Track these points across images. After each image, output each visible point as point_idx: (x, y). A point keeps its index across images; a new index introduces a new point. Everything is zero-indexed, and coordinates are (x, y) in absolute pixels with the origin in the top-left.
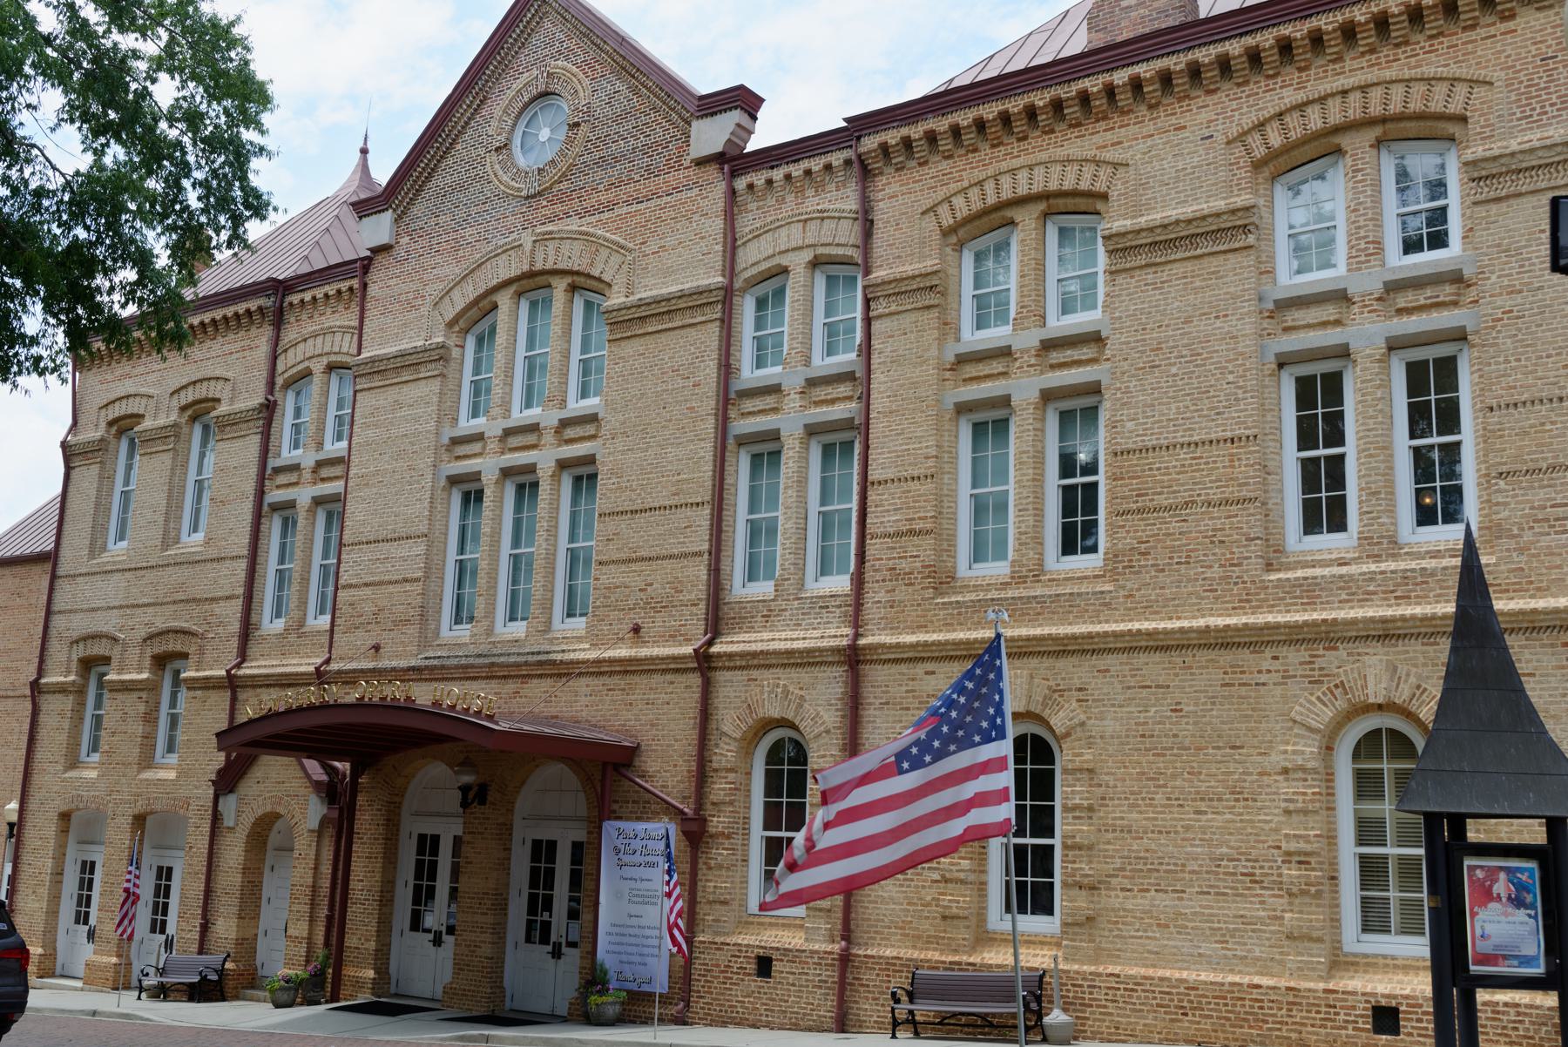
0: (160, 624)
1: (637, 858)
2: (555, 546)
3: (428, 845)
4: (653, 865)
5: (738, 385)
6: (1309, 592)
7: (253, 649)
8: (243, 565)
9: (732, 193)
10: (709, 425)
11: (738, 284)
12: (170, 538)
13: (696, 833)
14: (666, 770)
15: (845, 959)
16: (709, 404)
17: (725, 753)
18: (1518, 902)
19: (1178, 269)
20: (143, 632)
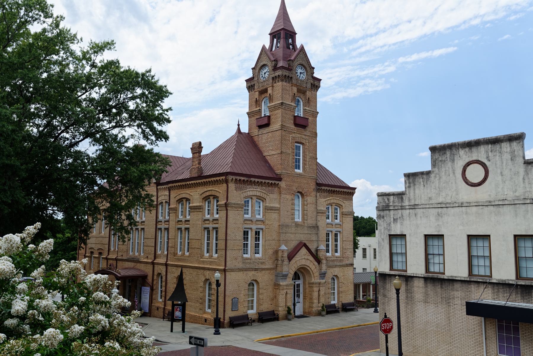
0: (99, 247)
3: (130, 287)
5: (158, 220)
6: (203, 262)
8: (108, 239)
9: (157, 189)
10: (155, 226)
12: (100, 232)
13: (152, 289)
14: (150, 279)
15: (164, 309)
16: (155, 223)
17: (155, 277)
20: (97, 248)
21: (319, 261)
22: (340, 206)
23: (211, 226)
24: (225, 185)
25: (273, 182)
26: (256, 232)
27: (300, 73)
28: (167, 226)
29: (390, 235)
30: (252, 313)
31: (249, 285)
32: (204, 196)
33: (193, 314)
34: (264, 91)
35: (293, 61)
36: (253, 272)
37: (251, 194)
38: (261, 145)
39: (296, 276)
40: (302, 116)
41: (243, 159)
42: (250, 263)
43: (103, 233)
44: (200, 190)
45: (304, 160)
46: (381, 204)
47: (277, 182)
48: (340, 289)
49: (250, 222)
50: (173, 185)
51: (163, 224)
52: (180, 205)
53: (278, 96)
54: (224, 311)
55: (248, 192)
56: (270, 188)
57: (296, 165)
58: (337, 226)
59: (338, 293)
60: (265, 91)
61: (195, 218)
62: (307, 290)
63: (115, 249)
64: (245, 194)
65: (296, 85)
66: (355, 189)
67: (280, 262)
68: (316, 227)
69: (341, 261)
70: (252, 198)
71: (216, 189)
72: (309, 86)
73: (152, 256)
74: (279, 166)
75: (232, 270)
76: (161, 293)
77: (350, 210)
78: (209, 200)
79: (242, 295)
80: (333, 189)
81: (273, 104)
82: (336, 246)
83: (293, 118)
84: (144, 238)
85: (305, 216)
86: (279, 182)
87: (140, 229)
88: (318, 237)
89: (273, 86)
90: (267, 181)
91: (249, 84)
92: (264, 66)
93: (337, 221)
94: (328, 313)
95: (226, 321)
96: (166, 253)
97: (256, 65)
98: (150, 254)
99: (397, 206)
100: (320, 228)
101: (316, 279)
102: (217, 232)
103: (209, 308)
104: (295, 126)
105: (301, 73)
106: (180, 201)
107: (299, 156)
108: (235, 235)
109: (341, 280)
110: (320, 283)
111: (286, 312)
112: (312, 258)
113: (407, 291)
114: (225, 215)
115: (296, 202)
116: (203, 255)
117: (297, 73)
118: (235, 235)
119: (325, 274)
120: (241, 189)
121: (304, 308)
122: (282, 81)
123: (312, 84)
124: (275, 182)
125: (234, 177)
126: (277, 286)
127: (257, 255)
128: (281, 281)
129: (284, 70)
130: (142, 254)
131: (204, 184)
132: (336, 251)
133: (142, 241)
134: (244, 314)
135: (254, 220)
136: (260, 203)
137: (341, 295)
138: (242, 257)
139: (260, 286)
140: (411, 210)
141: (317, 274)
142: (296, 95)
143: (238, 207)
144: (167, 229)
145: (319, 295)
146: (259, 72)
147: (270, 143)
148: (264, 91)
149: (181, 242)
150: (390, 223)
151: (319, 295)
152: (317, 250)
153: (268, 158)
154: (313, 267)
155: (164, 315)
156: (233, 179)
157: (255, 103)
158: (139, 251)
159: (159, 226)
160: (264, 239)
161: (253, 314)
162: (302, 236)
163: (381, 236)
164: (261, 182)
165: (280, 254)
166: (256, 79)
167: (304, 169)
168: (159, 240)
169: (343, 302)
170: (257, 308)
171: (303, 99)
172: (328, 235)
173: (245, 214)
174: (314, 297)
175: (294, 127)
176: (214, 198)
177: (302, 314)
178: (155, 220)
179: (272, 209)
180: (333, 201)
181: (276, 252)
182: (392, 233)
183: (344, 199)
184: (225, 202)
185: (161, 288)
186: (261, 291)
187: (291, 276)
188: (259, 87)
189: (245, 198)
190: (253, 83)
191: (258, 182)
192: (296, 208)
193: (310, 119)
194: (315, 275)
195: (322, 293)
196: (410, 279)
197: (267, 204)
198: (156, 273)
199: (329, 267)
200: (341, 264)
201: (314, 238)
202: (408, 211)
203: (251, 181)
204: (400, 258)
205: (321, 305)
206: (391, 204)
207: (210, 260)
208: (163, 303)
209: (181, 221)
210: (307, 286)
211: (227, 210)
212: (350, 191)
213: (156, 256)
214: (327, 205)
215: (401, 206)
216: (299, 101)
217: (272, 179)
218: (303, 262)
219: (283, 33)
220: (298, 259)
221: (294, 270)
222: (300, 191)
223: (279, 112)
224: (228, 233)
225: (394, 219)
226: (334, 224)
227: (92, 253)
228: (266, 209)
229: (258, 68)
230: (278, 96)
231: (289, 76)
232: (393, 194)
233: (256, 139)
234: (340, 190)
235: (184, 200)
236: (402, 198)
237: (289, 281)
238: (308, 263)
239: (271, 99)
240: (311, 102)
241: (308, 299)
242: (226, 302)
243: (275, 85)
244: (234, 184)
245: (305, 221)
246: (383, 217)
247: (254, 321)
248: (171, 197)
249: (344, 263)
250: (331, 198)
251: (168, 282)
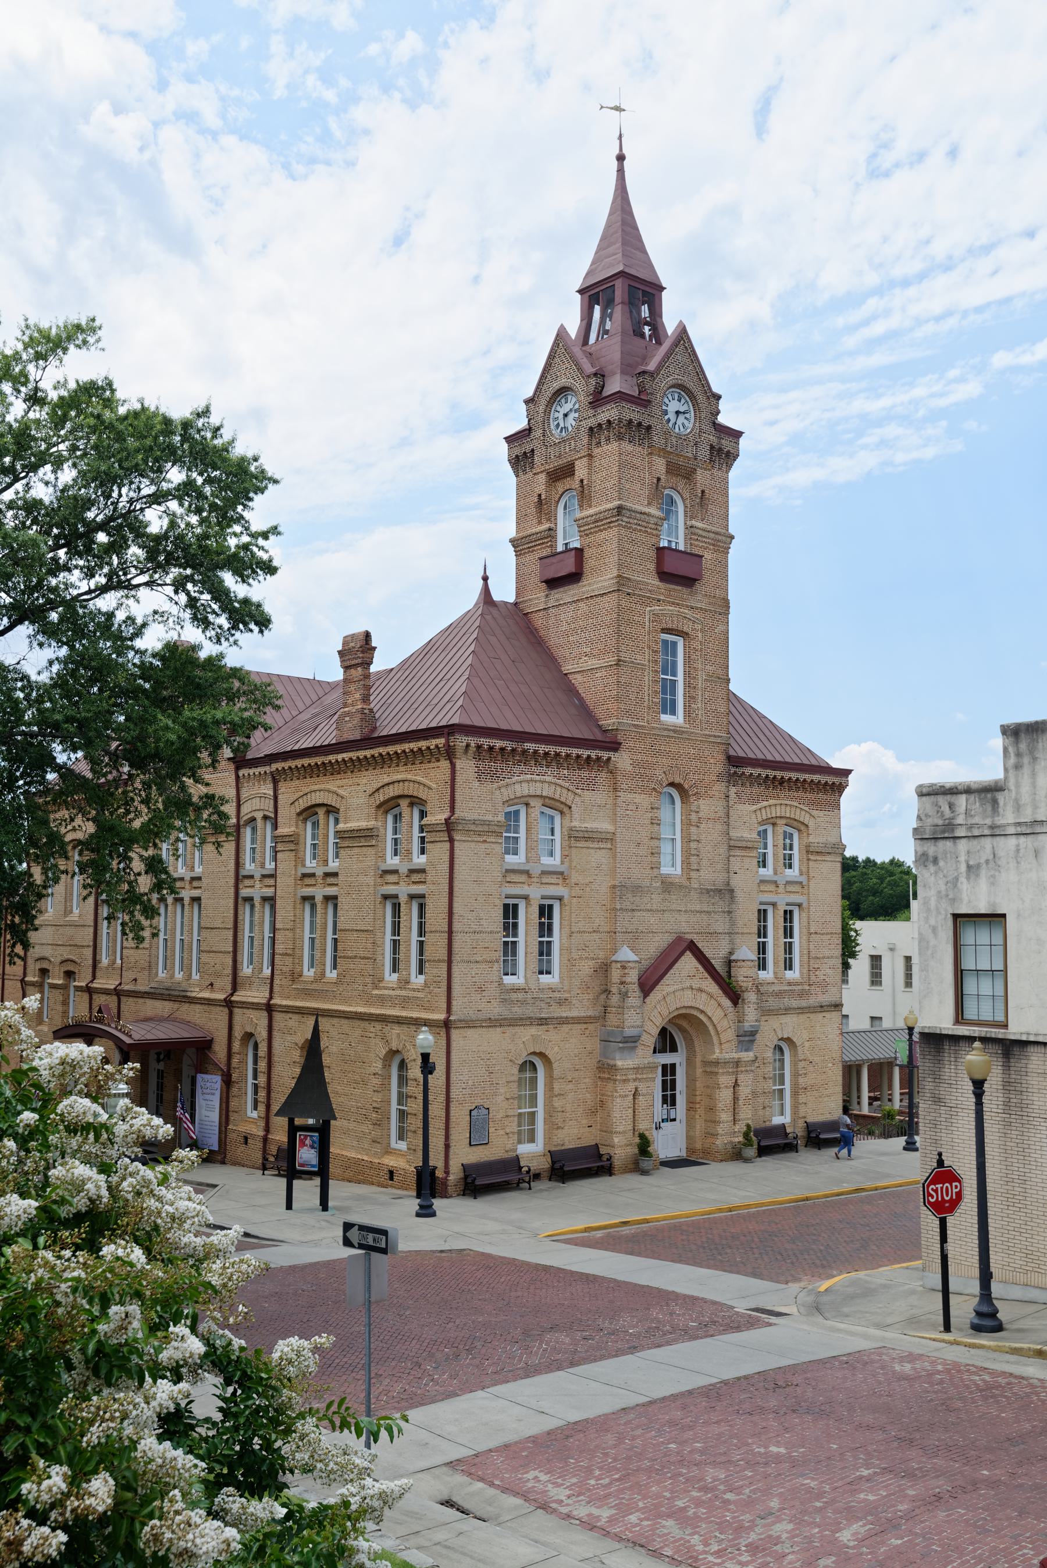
1: (208, 1091)
2: (192, 938)
3: (161, 1074)
4: (213, 1094)
5: (243, 872)
6: (382, 1000)
7: (98, 974)
8: (92, 930)
9: (237, 777)
10: (232, 890)
11: (242, 823)
12: (68, 911)
13: (228, 1082)
14: (219, 1051)
15: (265, 1140)
16: (232, 881)
17: (236, 1046)
18: (312, 1147)
19: (357, 850)
20: (59, 959)
21: (735, 996)
22: (801, 826)
23: (403, 890)
24: (445, 764)
25: (593, 754)
26: (542, 908)
27: (676, 413)
28: (269, 892)
29: (956, 916)
30: (532, 1152)
31: (522, 1067)
32: (381, 797)
33: (352, 1154)
34: (563, 473)
35: (652, 375)
36: (534, 1030)
37: (526, 792)
38: (554, 640)
39: (666, 1042)
40: (681, 547)
41: (500, 683)
42: (523, 1002)
43: (76, 911)
44: (370, 780)
45: (688, 685)
46: (929, 821)
47: (605, 755)
48: (801, 1080)
49: (523, 878)
50: (286, 765)
51: (258, 885)
52: (309, 825)
53: (609, 485)
54: (447, 1147)
55: (517, 786)
56: (585, 774)
57: (664, 700)
58: (790, 888)
59: (795, 1094)
60: (567, 471)
61: (354, 867)
62: (698, 1084)
63: (114, 962)
64: (507, 793)
65: (663, 452)
66: (847, 773)
67: (615, 999)
68: (727, 892)
69: (802, 994)
70: (527, 805)
71: (418, 778)
72: (704, 453)
73: (226, 983)
74: (612, 706)
75: (469, 1024)
76: (256, 1092)
77: (833, 840)
78: (396, 811)
79: (502, 1098)
80: (779, 774)
81: (591, 511)
82: (789, 948)
83: (653, 554)
84: (200, 928)
85: (693, 859)
86: (611, 754)
87: (187, 901)
88: (733, 923)
89: (590, 456)
90: (575, 751)
91: (518, 451)
92: (563, 391)
93: (793, 873)
94: (764, 1151)
95: (451, 1177)
96: (267, 972)
97: (538, 389)
98: (218, 975)
99: (979, 826)
100: (738, 893)
101: (725, 1050)
102: (422, 907)
103: (401, 1137)
104: (661, 580)
105: (678, 413)
106: (308, 813)
107: (674, 674)
108: (479, 918)
109: (804, 1051)
110: (737, 1063)
111: (636, 1151)
112: (713, 988)
113: (1008, 1085)
114: (446, 858)
115: (665, 814)
116: (382, 980)
117: (666, 413)
118: (479, 918)
119: (753, 1033)
120: (494, 777)
121: (688, 1137)
122: (620, 438)
123: (712, 447)
124: (601, 753)
125: (473, 741)
126: (605, 1071)
127: (545, 979)
128: (618, 1056)
129: (626, 401)
130: (195, 976)
131: (383, 761)
132: (789, 965)
133: (195, 937)
134: (506, 1156)
135: (536, 871)
136: (552, 818)
137: (802, 1099)
138: (500, 983)
139: (556, 1073)
140: (1022, 839)
141: (729, 1035)
142: (662, 483)
143: (485, 830)
144: (270, 901)
145: (735, 1099)
146: (547, 412)
147: (581, 634)
148: (563, 473)
149: (312, 940)
150: (957, 879)
151: (735, 1099)
152: (729, 963)
153: (577, 680)
154: (716, 1015)
155: (265, 1159)
156: (468, 746)
157: (537, 508)
158: (185, 967)
159: (244, 892)
160: (566, 930)
161: (533, 1157)
162: (683, 918)
163: (927, 919)
164: (557, 755)
165: (615, 974)
166: (537, 433)
167: (688, 713)
168: (247, 934)
169: (810, 1119)
170: (548, 1138)
171: (687, 495)
172: (762, 915)
173: (507, 852)
174: (720, 1105)
175: (656, 582)
176: (411, 805)
177: (684, 1154)
178: (232, 873)
179: (588, 837)
180: (778, 811)
181: (604, 968)
182: (964, 910)
183: (812, 803)
184: (446, 815)
185: (255, 1077)
186: (557, 1086)
187: (650, 1039)
188: (547, 458)
189: (508, 802)
190: (527, 448)
191: (546, 754)
192: (665, 833)
193: (708, 556)
194: (724, 1037)
195: (744, 1091)
196: (1016, 1050)
197: (575, 824)
198: (238, 1033)
199: (766, 1012)
200: (804, 1003)
201: (720, 924)
202: (1012, 841)
203: (524, 752)
204: (986, 987)
205: (740, 1127)
206: (960, 820)
207: (403, 993)
208: (262, 1124)
209: (313, 875)
210: (699, 1071)
211: (451, 841)
212: (830, 779)
213: (239, 980)
214: (761, 824)
215: (992, 827)
216: (672, 501)
217: (589, 747)
218: (687, 999)
219: (624, 289)
220: (671, 989)
221: (660, 1023)
222: (677, 780)
223: (611, 536)
224: (455, 910)
225: (969, 867)
226: (781, 882)
227: (44, 972)
228: (574, 837)
229: (545, 398)
230: (609, 485)
231: (640, 424)
232: (968, 791)
233: (538, 621)
234: (802, 776)
235: (321, 812)
236: (995, 802)
237: (644, 1055)
238: (701, 1002)
239: (584, 495)
240: (710, 503)
241: (701, 1111)
242: (453, 1119)
243: (596, 451)
244: (472, 763)
245: (693, 874)
246: (935, 861)
247: (537, 1176)
248: (280, 803)
249: (812, 1001)
250: (772, 802)
251: (275, 1059)
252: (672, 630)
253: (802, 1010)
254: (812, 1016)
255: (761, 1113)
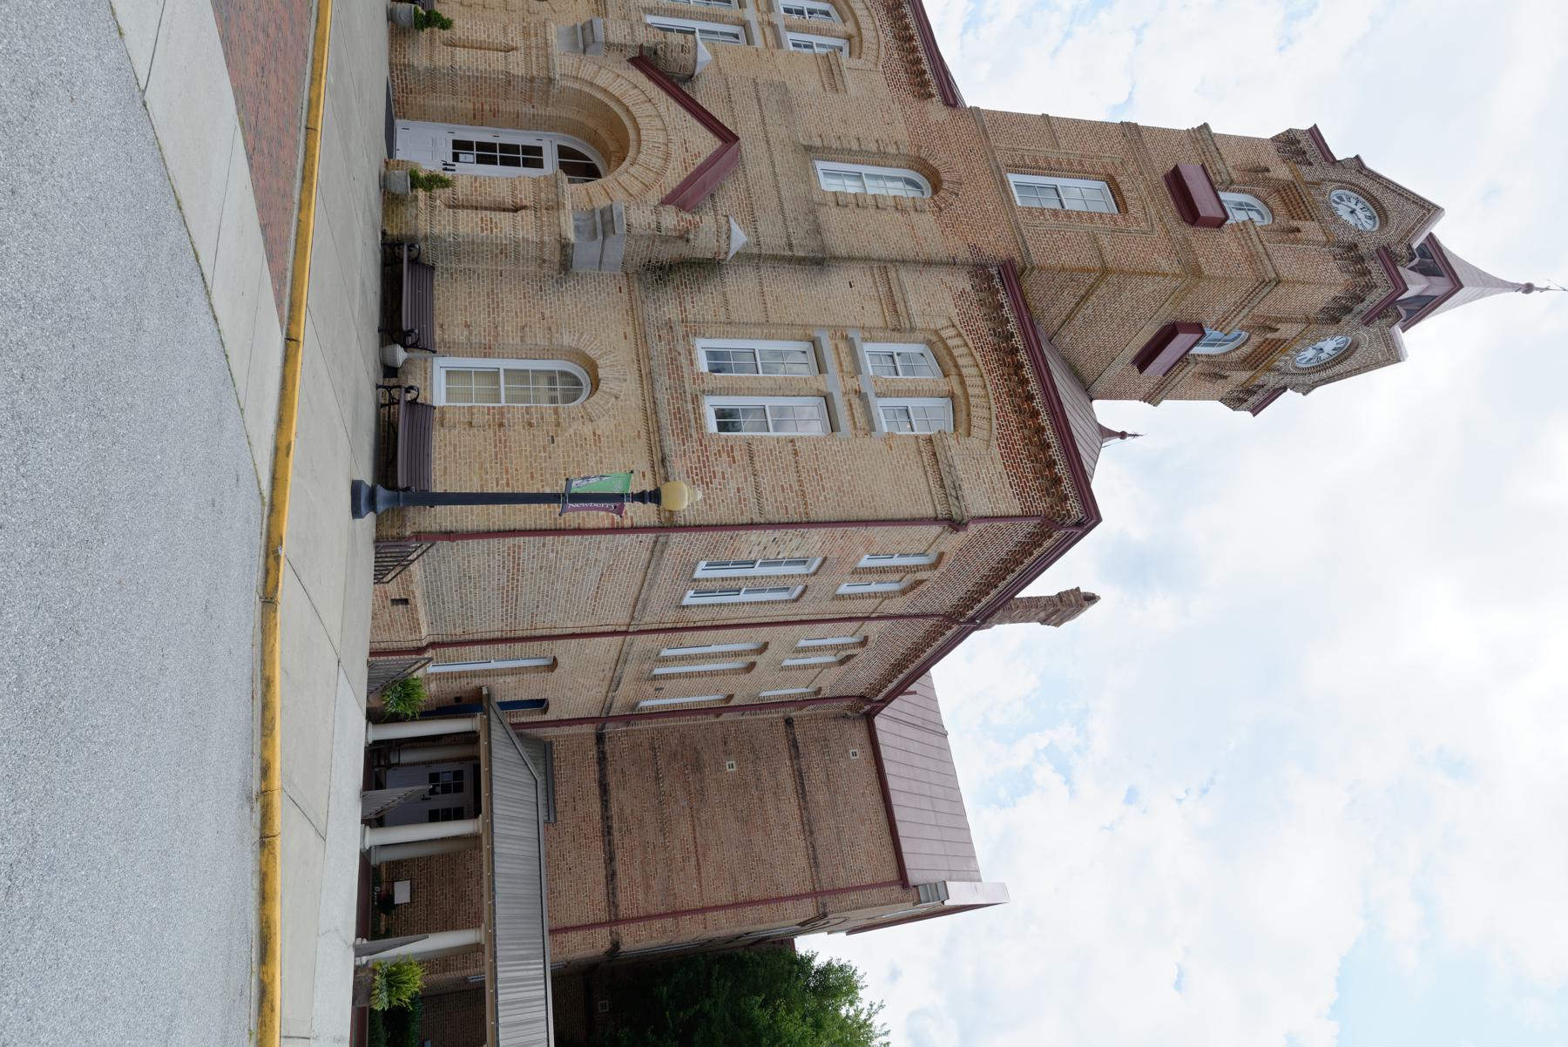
47: (934, 89)
56: (904, 77)
86: (937, 98)
124: (934, 83)
162: (765, 169)
183: (1007, 446)
200: (665, 418)
218: (651, 135)
220: (662, 110)
249: (671, 443)
252: (1121, 193)
253: (651, 412)
254: (643, 441)
255: (459, 319)
